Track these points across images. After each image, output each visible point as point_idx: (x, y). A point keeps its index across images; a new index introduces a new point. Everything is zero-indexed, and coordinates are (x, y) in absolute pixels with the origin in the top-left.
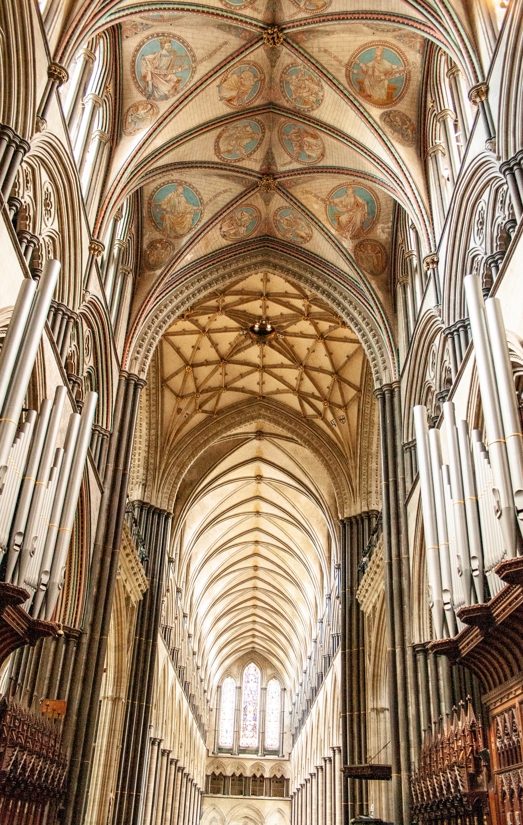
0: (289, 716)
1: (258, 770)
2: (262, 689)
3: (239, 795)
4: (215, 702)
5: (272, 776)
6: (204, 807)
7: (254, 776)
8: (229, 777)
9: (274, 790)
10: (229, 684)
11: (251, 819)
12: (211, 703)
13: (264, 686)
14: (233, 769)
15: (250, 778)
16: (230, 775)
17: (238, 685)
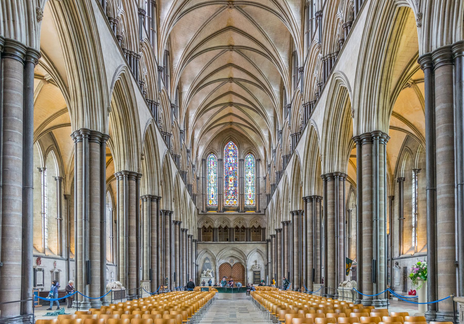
0: (264, 181)
1: (240, 223)
2: (240, 160)
3: (226, 241)
4: (201, 172)
5: (251, 226)
6: (199, 251)
7: (237, 228)
8: (217, 229)
9: (253, 237)
10: (212, 161)
11: (236, 258)
12: (198, 173)
13: (242, 158)
14: (220, 223)
15: (233, 229)
16: (218, 227)
17: (220, 157)
